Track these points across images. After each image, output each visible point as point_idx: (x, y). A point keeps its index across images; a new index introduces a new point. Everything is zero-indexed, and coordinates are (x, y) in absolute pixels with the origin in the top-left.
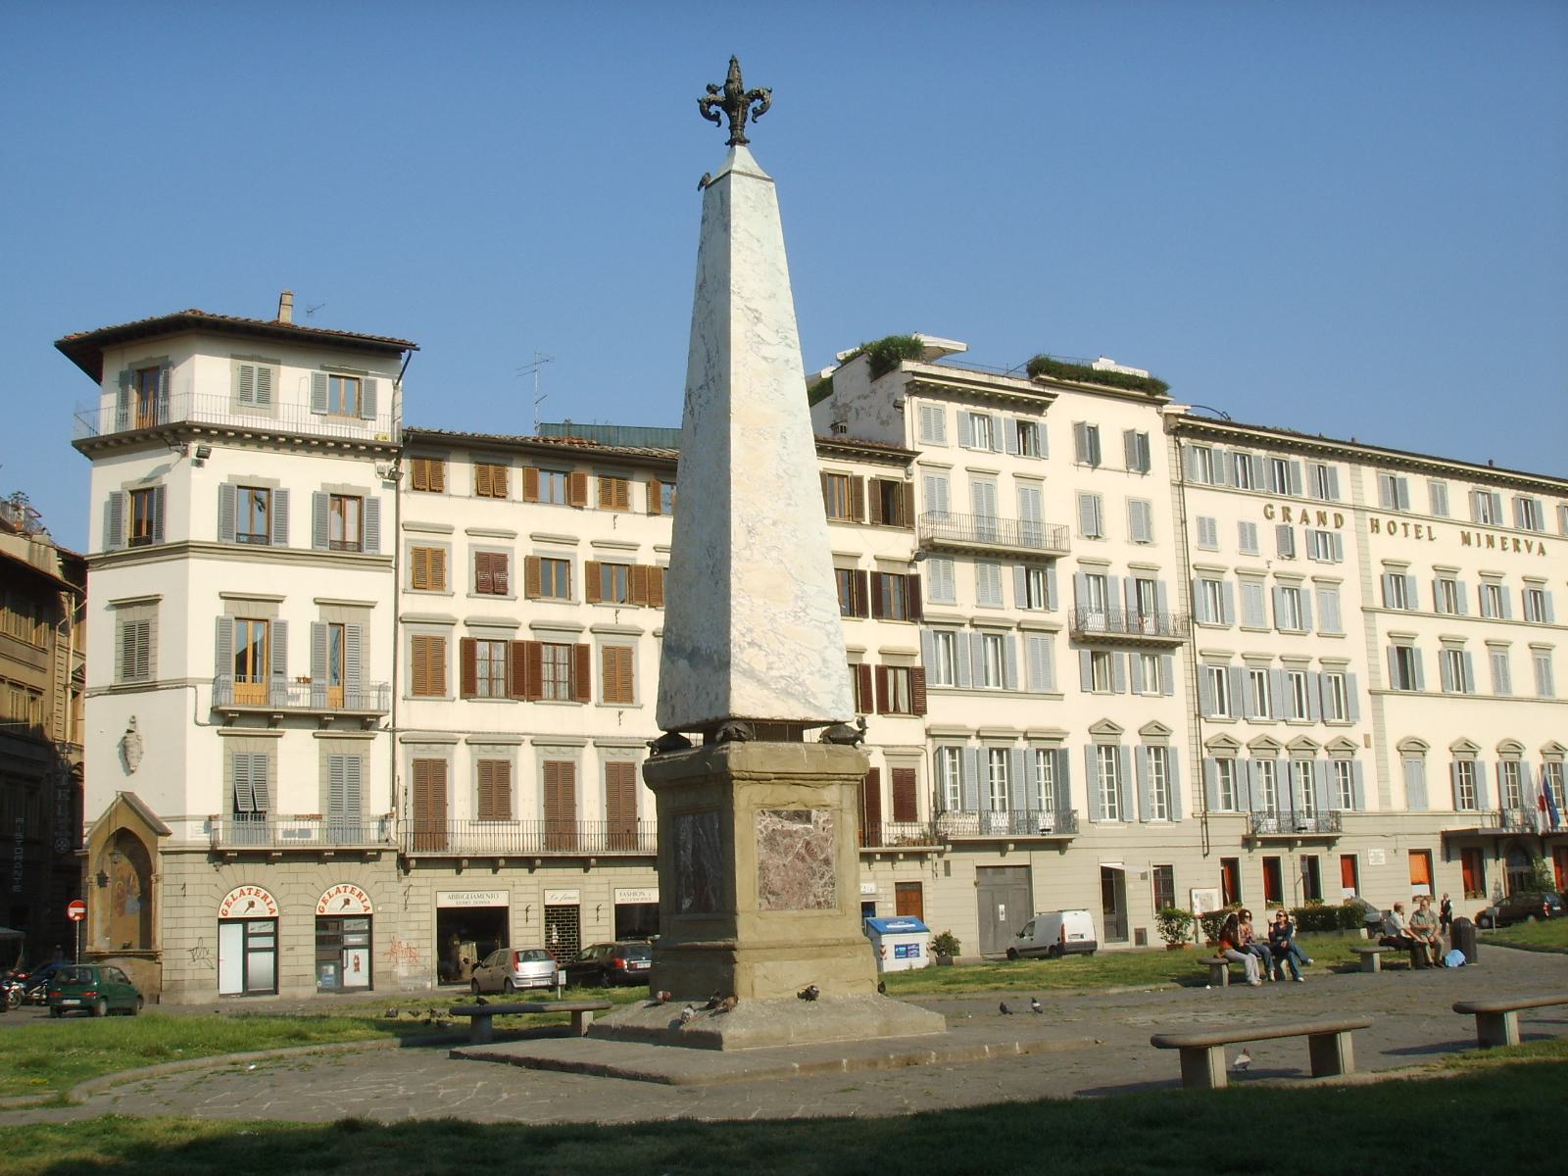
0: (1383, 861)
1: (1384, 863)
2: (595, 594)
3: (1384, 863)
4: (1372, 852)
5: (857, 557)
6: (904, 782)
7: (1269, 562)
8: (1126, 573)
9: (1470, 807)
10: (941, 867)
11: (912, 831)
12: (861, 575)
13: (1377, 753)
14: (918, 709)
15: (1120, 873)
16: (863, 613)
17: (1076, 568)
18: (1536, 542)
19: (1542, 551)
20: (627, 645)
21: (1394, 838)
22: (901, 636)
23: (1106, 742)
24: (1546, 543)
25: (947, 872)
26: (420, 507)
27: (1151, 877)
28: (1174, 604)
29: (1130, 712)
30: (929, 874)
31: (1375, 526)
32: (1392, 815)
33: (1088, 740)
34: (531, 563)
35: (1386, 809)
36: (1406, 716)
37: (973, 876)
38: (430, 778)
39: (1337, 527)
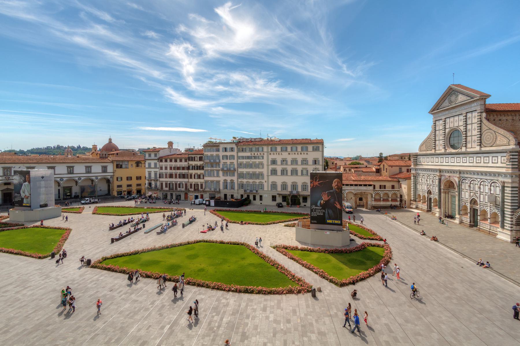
2: (174, 169)
4: (265, 195)
6: (202, 185)
8: (229, 163)
9: (285, 190)
11: (202, 190)
12: (198, 166)
14: (203, 178)
15: (226, 194)
16: (198, 170)
17: (223, 163)
18: (306, 153)
19: (307, 154)
22: (202, 171)
23: (225, 181)
24: (308, 152)
26: (161, 163)
28: (236, 167)
29: (229, 179)
31: (270, 154)
34: (174, 167)
36: (273, 179)
38: (162, 184)
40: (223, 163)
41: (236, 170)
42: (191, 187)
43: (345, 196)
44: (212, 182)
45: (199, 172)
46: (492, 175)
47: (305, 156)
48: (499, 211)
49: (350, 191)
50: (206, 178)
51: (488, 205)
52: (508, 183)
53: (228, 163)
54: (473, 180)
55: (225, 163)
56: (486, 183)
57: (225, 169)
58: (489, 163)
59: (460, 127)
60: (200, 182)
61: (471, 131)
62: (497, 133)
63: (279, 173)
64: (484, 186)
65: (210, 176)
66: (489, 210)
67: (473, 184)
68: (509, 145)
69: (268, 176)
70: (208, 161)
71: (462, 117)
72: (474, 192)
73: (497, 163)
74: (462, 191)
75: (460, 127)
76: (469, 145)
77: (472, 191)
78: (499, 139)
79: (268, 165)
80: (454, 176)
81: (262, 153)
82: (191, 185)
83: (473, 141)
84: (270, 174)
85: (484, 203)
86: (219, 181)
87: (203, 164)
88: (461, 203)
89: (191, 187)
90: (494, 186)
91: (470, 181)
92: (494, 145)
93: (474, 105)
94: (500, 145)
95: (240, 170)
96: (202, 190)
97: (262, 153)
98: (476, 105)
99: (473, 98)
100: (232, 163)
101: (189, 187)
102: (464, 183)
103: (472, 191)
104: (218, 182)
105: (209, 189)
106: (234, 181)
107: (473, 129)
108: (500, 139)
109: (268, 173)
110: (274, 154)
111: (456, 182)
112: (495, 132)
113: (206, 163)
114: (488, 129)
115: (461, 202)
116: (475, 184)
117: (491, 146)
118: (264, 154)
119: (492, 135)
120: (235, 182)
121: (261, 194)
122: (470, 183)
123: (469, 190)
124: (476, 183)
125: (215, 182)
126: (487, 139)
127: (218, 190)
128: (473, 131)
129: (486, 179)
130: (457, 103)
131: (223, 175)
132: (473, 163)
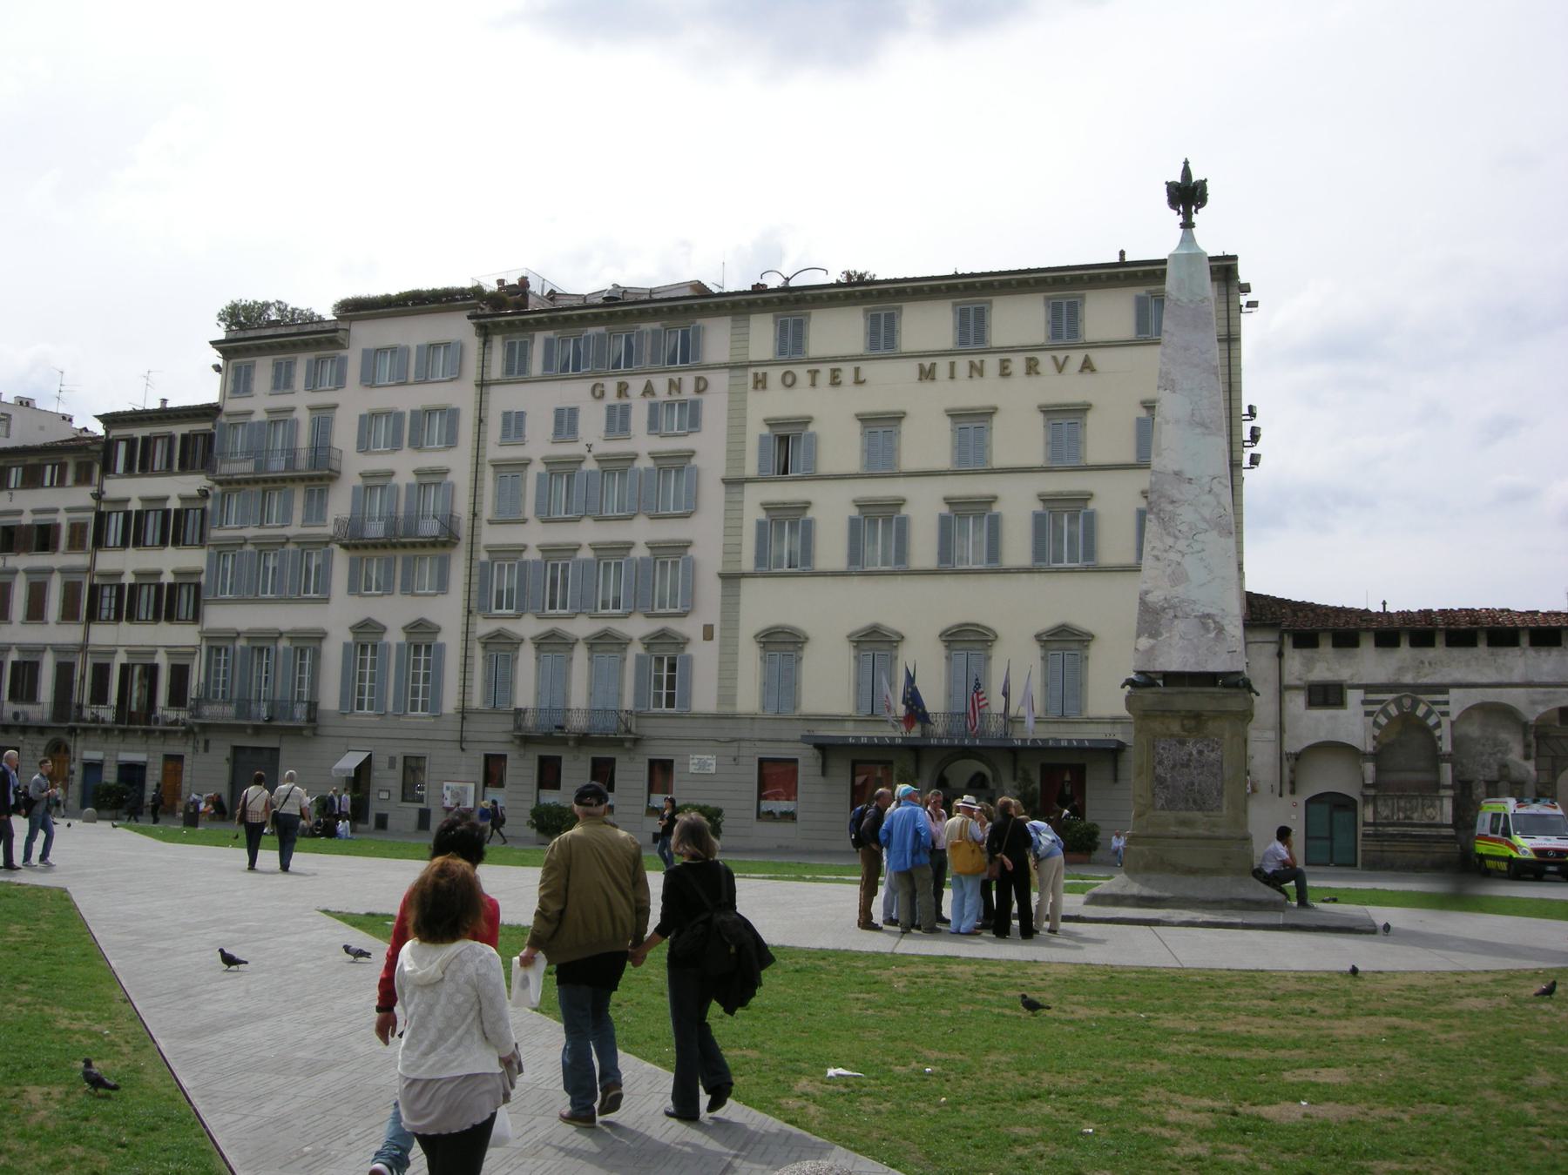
0: (713, 769)
1: (714, 771)
3: (714, 771)
5: (127, 500)
6: (180, 674)
7: (589, 446)
8: (413, 479)
10: (202, 744)
13: (721, 646)
14: (196, 618)
18: (1077, 357)
20: (6, 581)
21: (735, 744)
22: (192, 559)
25: (206, 749)
27: (399, 766)
30: (190, 750)
31: (760, 383)
32: (733, 717)
33: (349, 638)
35: (727, 710)
37: (227, 753)
39: (698, 391)
40: (359, 482)
41: (464, 531)
42: (99, 696)
43: (1446, 746)
44: (262, 642)
45: (169, 562)
47: (1067, 387)
49: (1491, 695)
50: (219, 617)
53: (404, 478)
55: (376, 481)
57: (376, 530)
60: (171, 651)
63: (831, 549)
65: (249, 596)
69: (731, 579)
70: (244, 468)
79: (734, 483)
81: (688, 380)
82: (101, 672)
84: (748, 564)
86: (319, 637)
87: (204, 494)
89: (99, 696)
95: (492, 536)
96: (172, 715)
97: (688, 380)
100: (431, 479)
101: (83, 691)
104: (308, 643)
105: (231, 710)
106: (436, 630)
109: (731, 551)
110: (789, 382)
113: (231, 484)
118: (701, 387)
120: (441, 648)
121: (661, 752)
125: (283, 644)
127: (300, 712)
131: (353, 588)
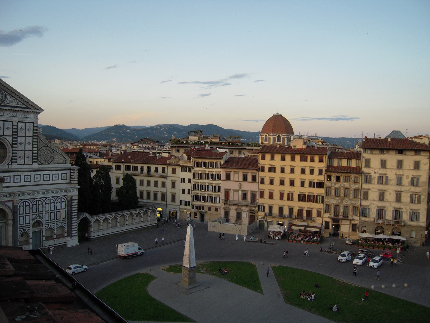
46: (59, 191)
48: (65, 223)
51: (54, 222)
52: (75, 196)
54: (36, 201)
56: (51, 200)
58: (49, 180)
59: (7, 138)
61: (24, 145)
62: (54, 151)
64: (50, 204)
66: (55, 226)
67: (36, 205)
68: (66, 164)
71: (9, 125)
72: (38, 213)
73: (58, 180)
74: (20, 216)
75: (7, 138)
76: (21, 161)
77: (34, 214)
78: (56, 157)
80: (4, 201)
83: (26, 157)
85: (50, 221)
88: (19, 232)
90: (60, 202)
91: (33, 203)
92: (52, 163)
93: (30, 116)
94: (61, 163)
98: (32, 117)
99: (28, 108)
102: (23, 206)
103: (34, 214)
107: (26, 142)
108: (58, 157)
111: (9, 207)
112: (53, 150)
114: (44, 146)
115: (19, 230)
116: (39, 204)
117: (49, 164)
119: (49, 153)
122: (33, 205)
123: (31, 212)
124: (40, 203)
126: (44, 156)
128: (26, 145)
129: (53, 197)
130: (3, 104)
132: (30, 181)
